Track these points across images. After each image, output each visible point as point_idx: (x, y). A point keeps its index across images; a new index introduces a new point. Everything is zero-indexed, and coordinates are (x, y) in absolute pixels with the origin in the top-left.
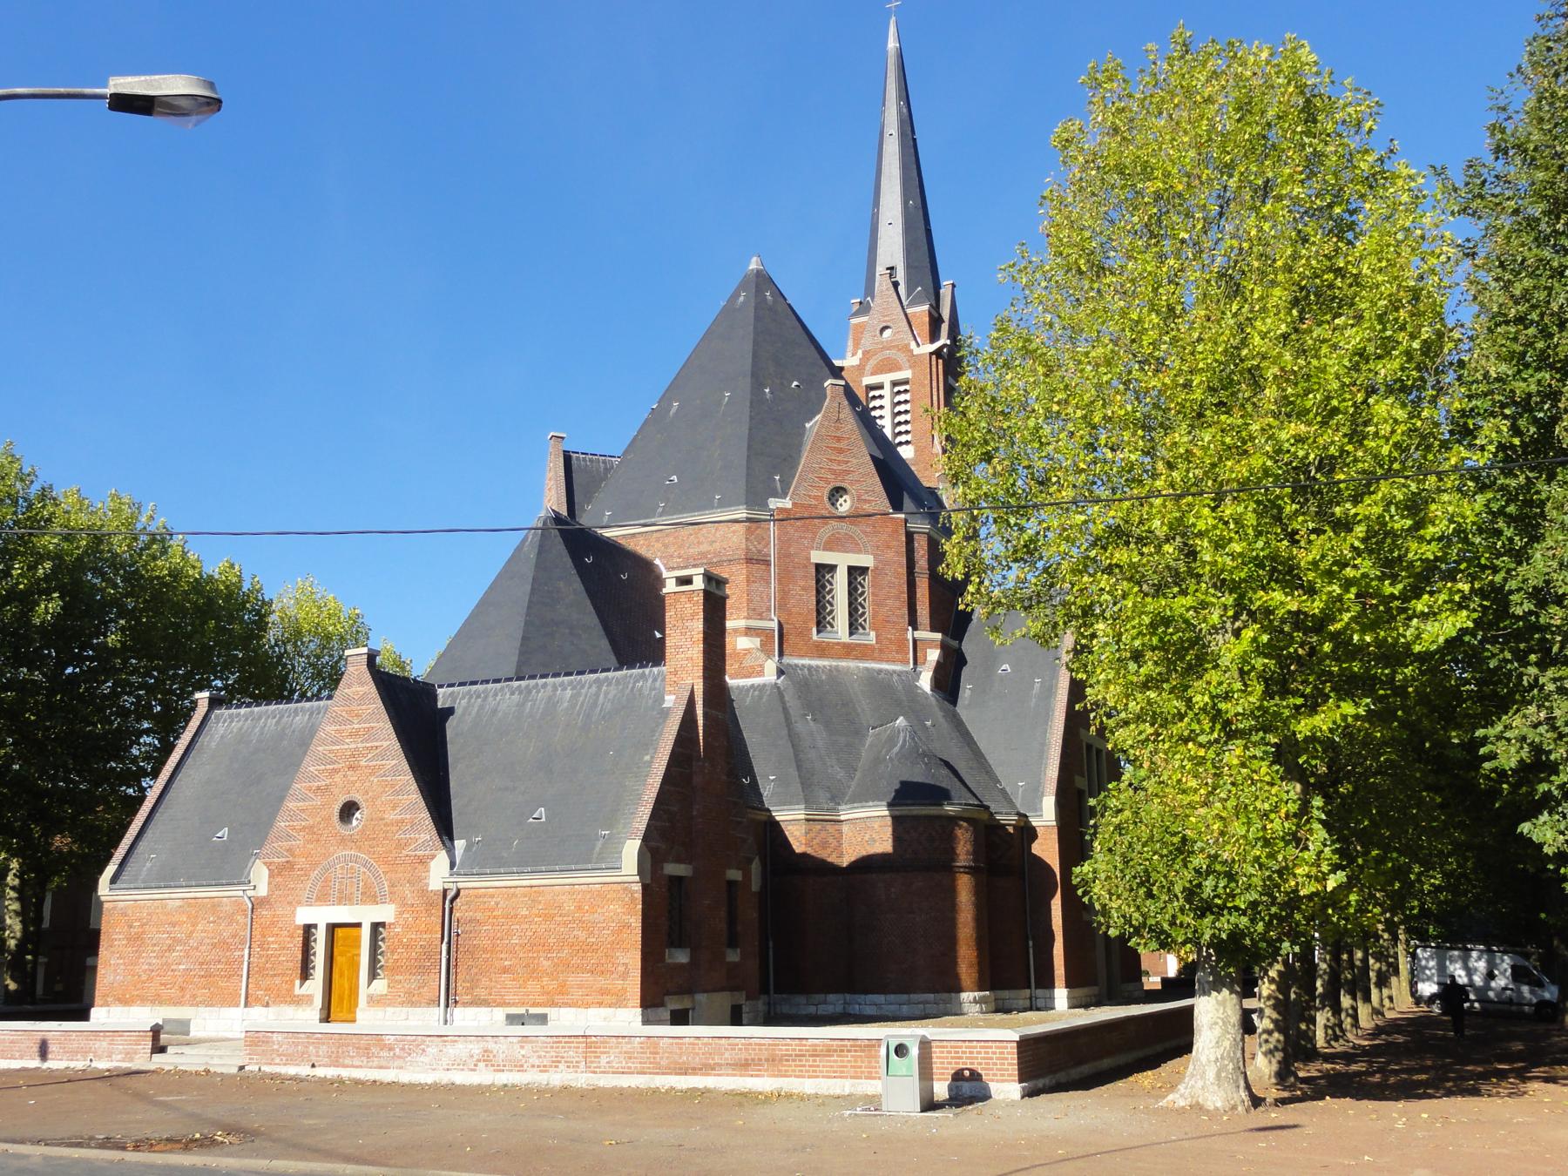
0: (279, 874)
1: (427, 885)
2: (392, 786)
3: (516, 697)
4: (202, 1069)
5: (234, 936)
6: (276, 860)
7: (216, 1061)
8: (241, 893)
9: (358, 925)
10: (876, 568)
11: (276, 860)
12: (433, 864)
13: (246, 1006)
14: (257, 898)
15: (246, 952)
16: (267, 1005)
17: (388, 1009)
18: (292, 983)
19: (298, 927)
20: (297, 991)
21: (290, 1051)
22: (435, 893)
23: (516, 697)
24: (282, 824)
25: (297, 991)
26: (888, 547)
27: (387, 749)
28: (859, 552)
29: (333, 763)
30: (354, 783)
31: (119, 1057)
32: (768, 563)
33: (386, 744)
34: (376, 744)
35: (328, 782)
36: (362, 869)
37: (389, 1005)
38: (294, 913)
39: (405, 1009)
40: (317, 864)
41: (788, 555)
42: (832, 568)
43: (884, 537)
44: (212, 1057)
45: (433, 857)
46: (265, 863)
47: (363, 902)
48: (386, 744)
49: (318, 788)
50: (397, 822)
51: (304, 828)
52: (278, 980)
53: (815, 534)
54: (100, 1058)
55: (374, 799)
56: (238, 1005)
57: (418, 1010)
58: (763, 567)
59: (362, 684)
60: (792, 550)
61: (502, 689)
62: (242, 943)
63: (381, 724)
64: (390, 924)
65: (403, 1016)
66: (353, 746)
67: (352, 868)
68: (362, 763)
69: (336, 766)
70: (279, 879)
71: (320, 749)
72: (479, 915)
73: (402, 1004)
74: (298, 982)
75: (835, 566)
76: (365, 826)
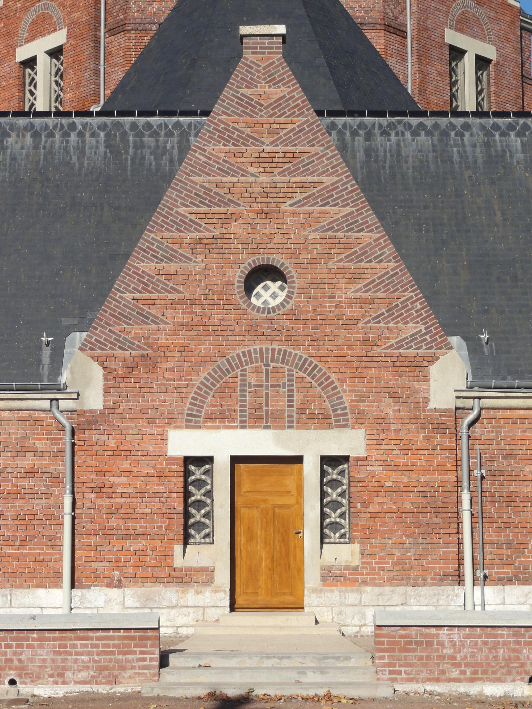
0: (127, 375)
1: (427, 401)
2: (348, 246)
3: (422, 137)
4: (321, 692)
5: (32, 473)
6: (118, 352)
7: (262, 677)
8: (46, 404)
9: (298, 460)
10: (498, 63)
11: (118, 352)
12: (434, 369)
13: (73, 586)
14: (82, 414)
15: (67, 499)
16: (120, 585)
17: (368, 589)
18: (170, 545)
19: (173, 460)
20: (178, 562)
21: (480, 657)
22: (442, 413)
23: (422, 137)
24: (128, 296)
25: (178, 562)
26: (508, 40)
27: (334, 187)
28: (484, 39)
29: (222, 202)
30: (271, 236)
31: (83, 675)
32: (403, 34)
33: (328, 180)
34: (310, 179)
35: (217, 233)
36: (297, 373)
37: (364, 583)
38: (164, 440)
39: (401, 589)
40: (205, 362)
41: (427, 29)
42: (462, 52)
43: (504, 27)
44: (302, 671)
45: (434, 359)
46: (95, 358)
47: (302, 425)
48: (328, 180)
49: (199, 242)
50: (363, 303)
51: (173, 304)
52: (136, 546)
53: (449, 7)
54: (35, 679)
55: (313, 262)
56: (57, 584)
57: (424, 590)
58: (399, 39)
59: (273, 82)
60: (430, 23)
61: (391, 126)
62: (56, 482)
63: (319, 149)
64: (358, 459)
65: (397, 599)
66: (264, 179)
67: (276, 371)
68: (285, 207)
69: (231, 209)
70: (129, 383)
71: (196, 179)
72: (520, 451)
73: (390, 580)
74: (178, 548)
75: (466, 51)
76: (297, 305)
